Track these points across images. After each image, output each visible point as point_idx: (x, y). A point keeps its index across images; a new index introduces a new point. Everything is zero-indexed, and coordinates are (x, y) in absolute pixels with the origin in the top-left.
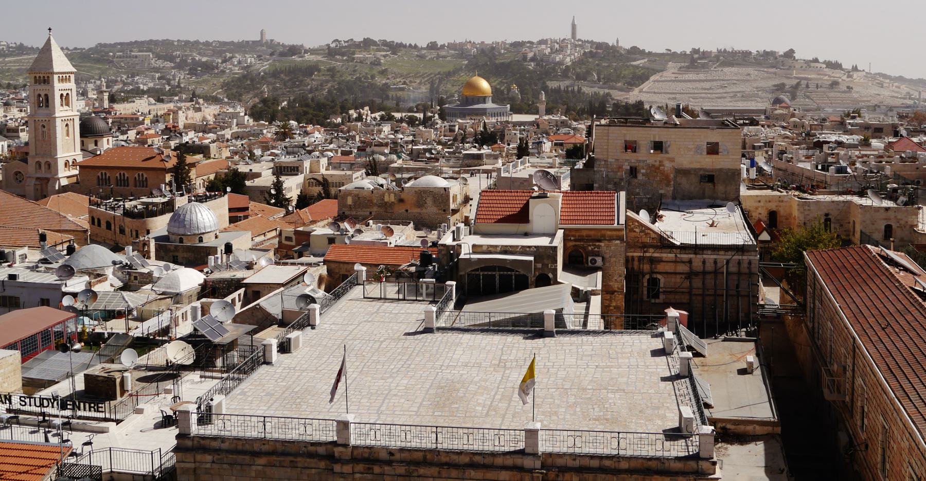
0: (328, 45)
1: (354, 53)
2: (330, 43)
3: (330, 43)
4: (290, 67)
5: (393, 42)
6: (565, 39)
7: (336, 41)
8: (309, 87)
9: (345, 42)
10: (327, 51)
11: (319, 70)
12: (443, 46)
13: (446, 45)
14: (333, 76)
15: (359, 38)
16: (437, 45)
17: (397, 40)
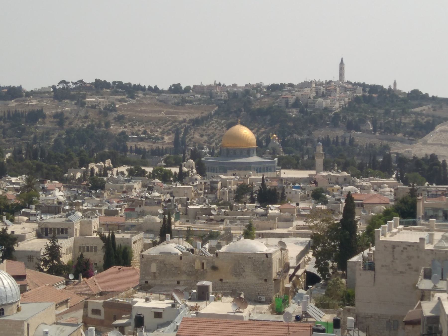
0: (54, 87)
1: (84, 97)
2: (56, 84)
3: (56, 84)
4: (9, 112)
5: (130, 84)
6: (330, 82)
7: (63, 82)
8: (32, 136)
9: (74, 84)
10: (53, 94)
11: (44, 117)
12: (188, 89)
13: (192, 87)
14: (61, 124)
15: (89, 80)
16: (181, 87)
17: (134, 81)
